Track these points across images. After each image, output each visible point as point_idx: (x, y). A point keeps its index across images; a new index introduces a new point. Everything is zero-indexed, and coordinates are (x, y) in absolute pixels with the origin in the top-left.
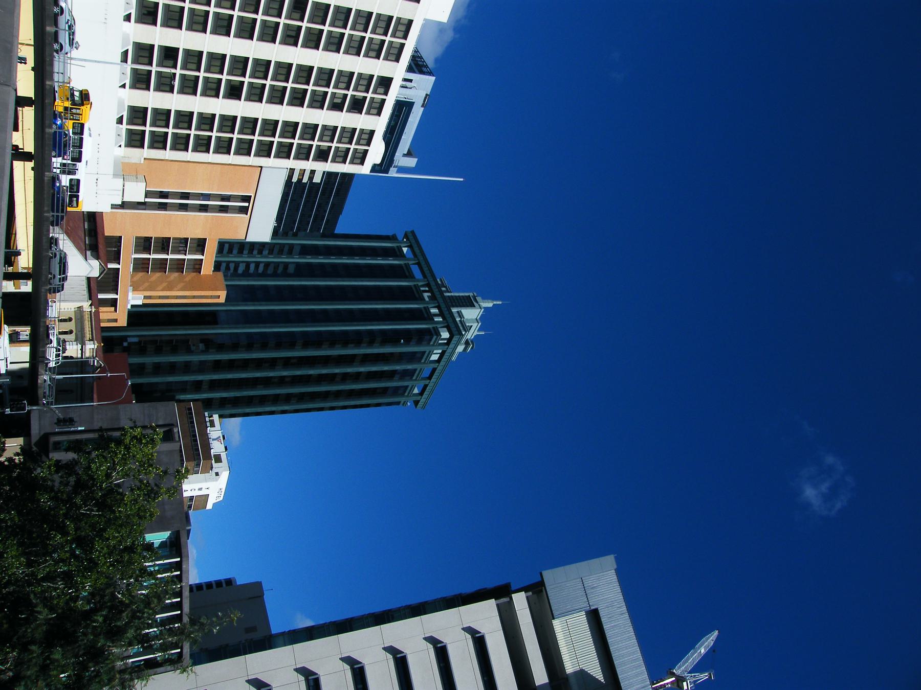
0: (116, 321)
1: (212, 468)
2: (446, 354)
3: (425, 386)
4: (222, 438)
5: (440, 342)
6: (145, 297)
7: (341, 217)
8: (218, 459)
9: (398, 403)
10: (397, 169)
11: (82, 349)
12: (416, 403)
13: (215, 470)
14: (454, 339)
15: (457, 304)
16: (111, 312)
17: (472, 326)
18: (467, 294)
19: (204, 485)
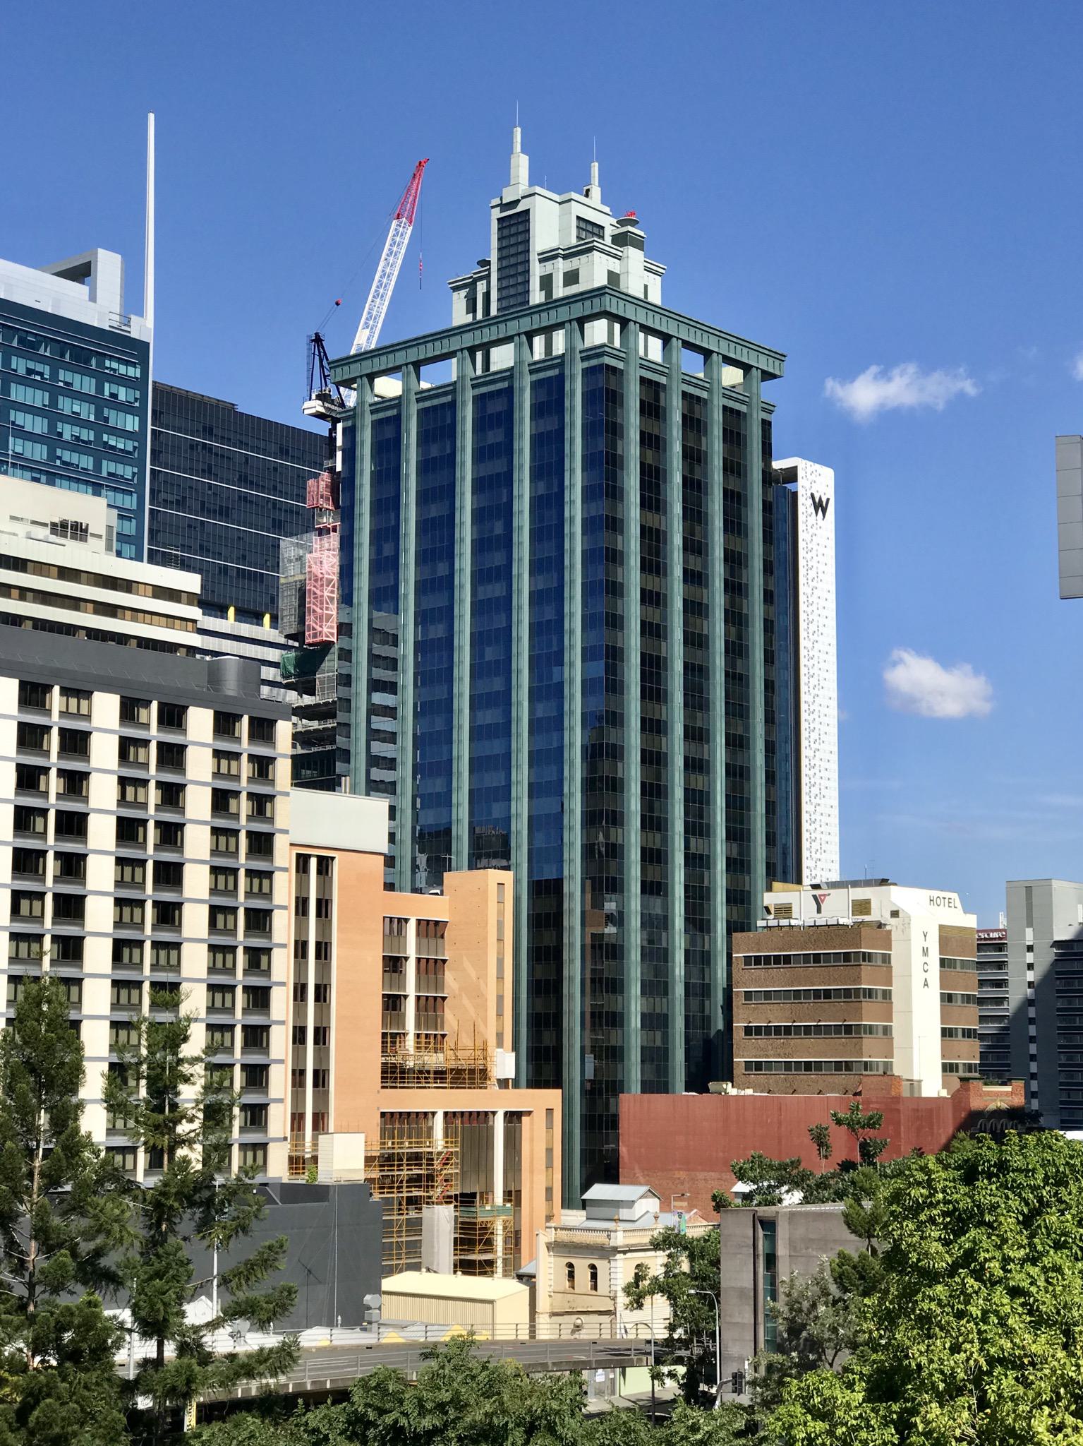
0: (550, 1111)
1: (880, 925)
2: (650, 324)
4: (817, 892)
5: (617, 344)
6: (500, 1044)
7: (240, 409)
8: (862, 907)
9: (766, 425)
10: (133, 317)
11: (624, 1252)
12: (767, 376)
13: (886, 918)
14: (614, 311)
15: (520, 269)
16: (532, 1123)
17: (578, 218)
18: (494, 226)
19: (917, 944)
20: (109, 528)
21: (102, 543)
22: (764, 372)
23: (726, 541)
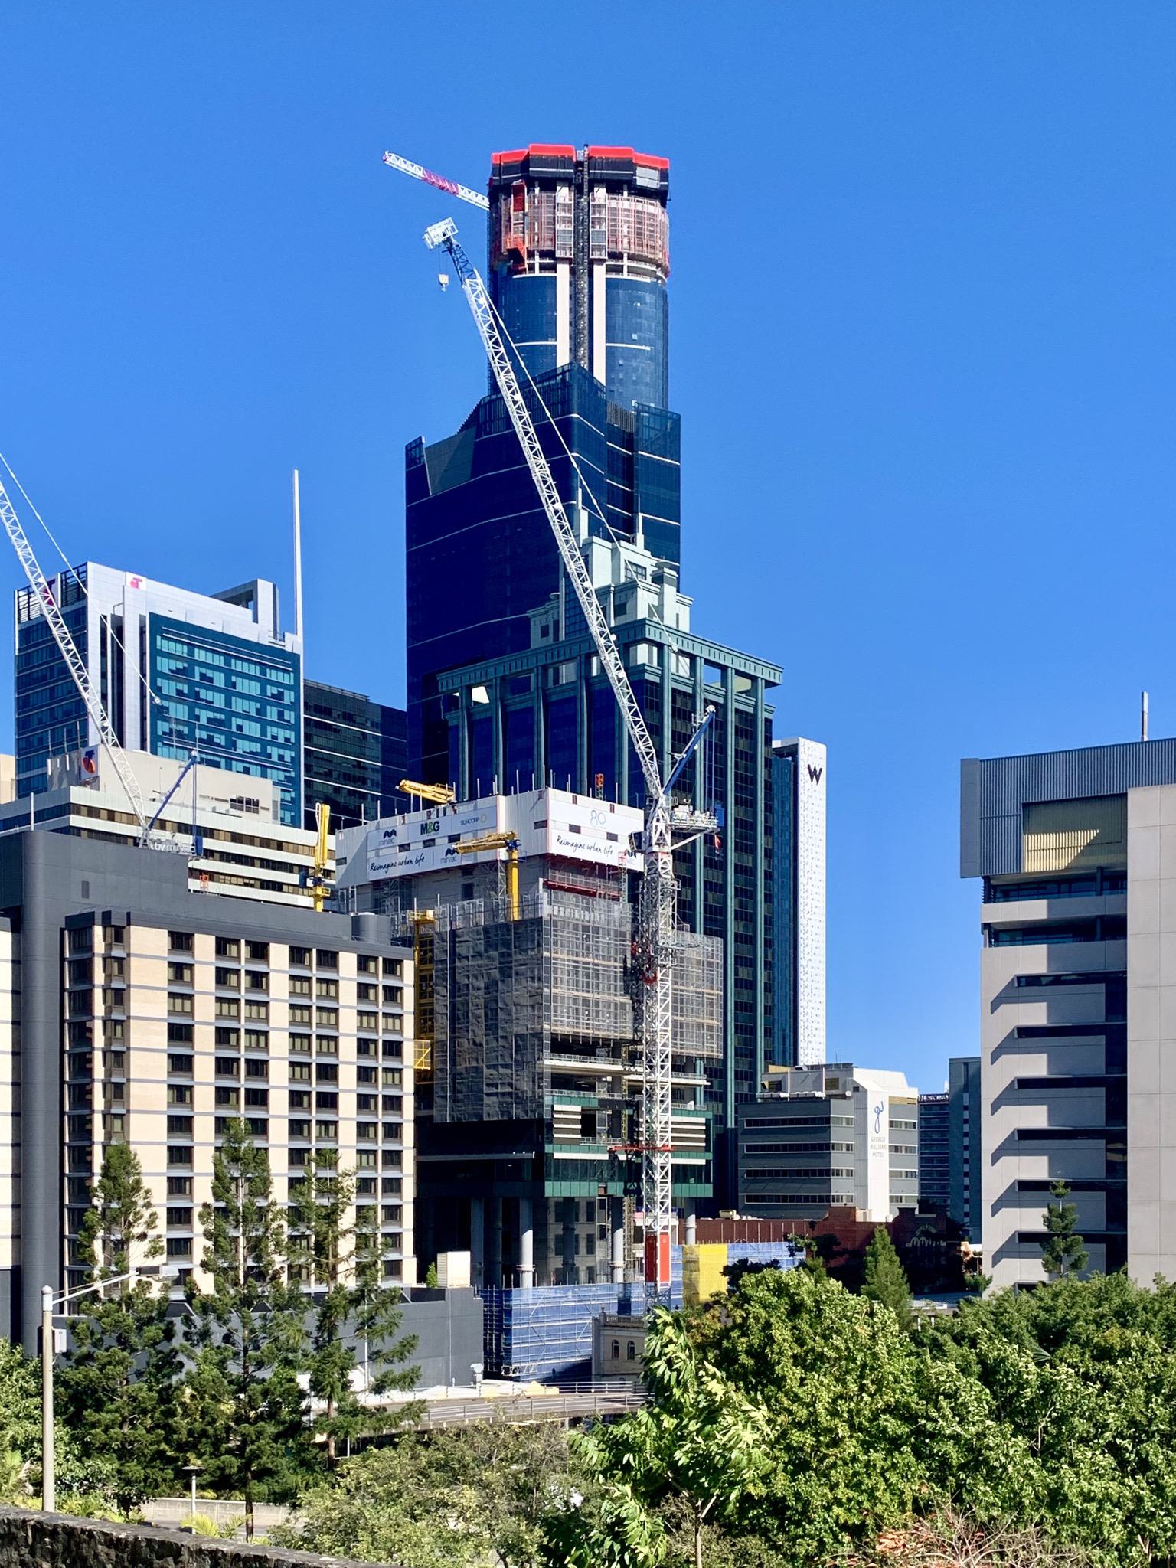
3: (738, 673)
5: (655, 664)
9: (768, 722)
20: (275, 802)
21: (270, 814)
22: (766, 681)
23: (706, 875)
